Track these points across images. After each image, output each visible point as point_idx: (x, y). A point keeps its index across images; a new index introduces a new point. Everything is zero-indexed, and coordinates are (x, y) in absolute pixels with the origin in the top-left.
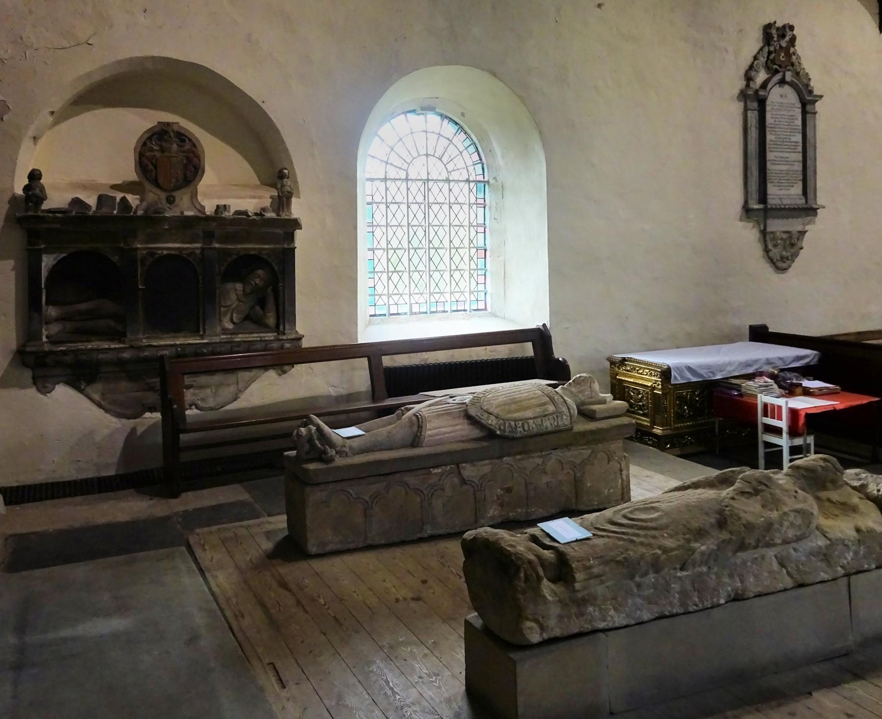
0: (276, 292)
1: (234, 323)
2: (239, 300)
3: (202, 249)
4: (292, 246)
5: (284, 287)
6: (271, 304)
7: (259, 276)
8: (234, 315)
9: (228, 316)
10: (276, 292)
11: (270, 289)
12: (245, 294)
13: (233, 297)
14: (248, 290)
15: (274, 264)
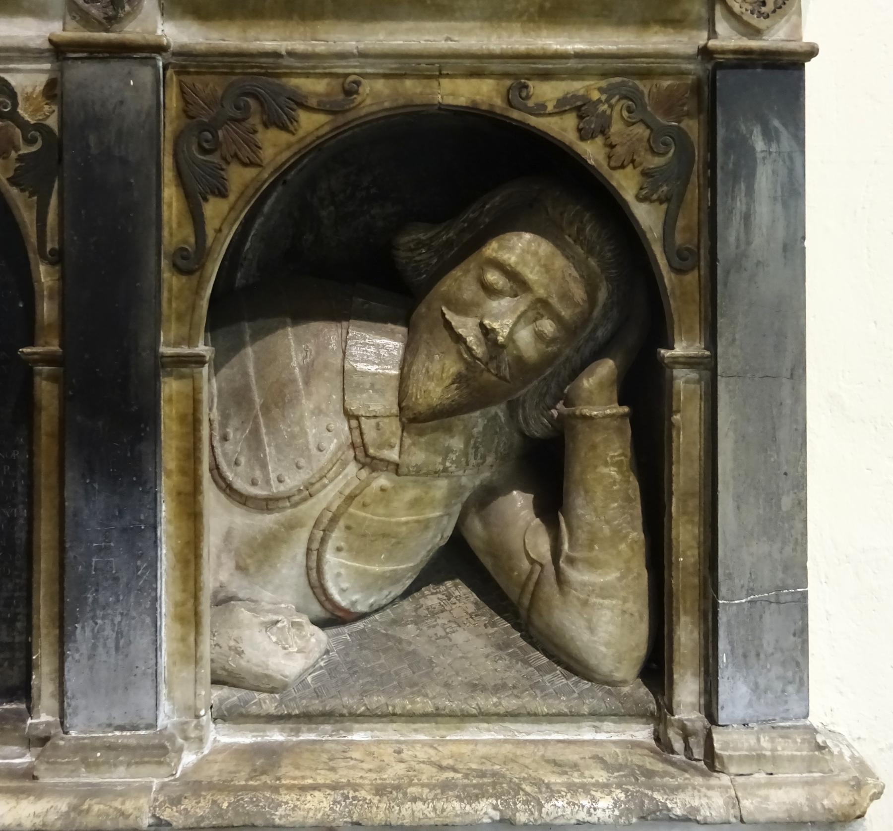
0: (645, 396)
1: (333, 618)
2: (370, 463)
3: (59, 50)
4: (776, 37)
5: (708, 368)
6: (604, 479)
7: (518, 283)
8: (334, 562)
9: (290, 567)
10: (645, 396)
11: (597, 389)
12: (414, 419)
13: (319, 431)
14: (436, 382)
15: (626, 183)
